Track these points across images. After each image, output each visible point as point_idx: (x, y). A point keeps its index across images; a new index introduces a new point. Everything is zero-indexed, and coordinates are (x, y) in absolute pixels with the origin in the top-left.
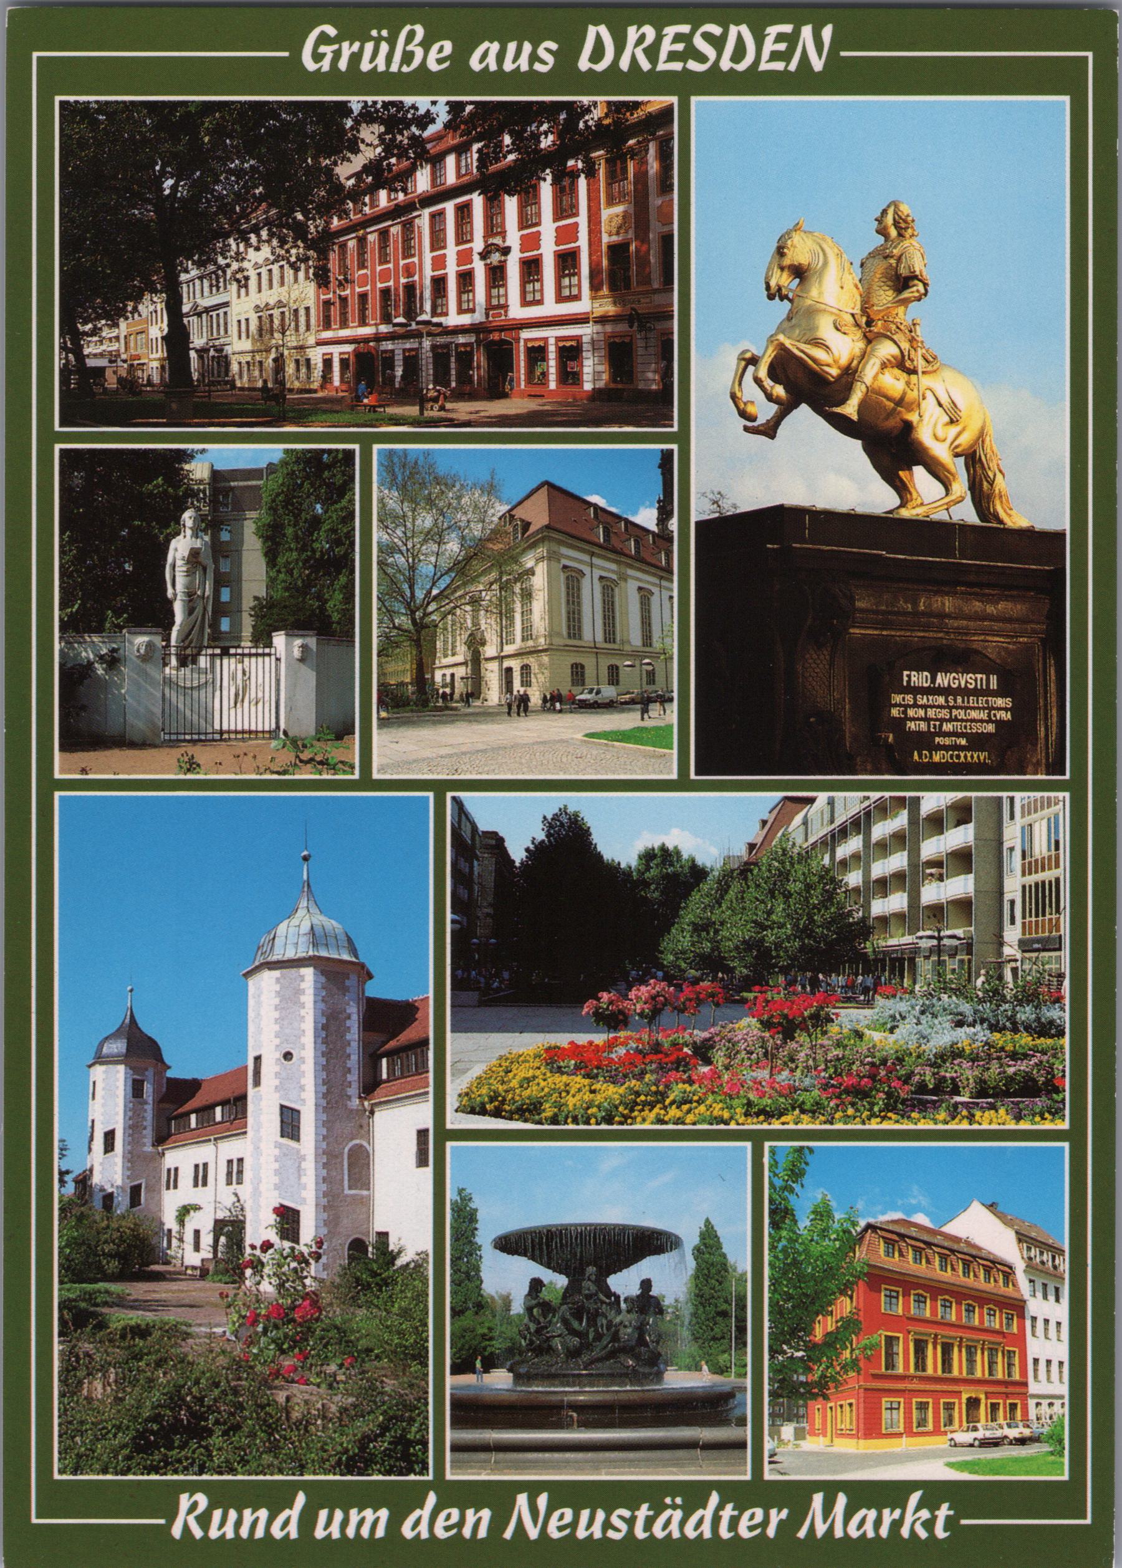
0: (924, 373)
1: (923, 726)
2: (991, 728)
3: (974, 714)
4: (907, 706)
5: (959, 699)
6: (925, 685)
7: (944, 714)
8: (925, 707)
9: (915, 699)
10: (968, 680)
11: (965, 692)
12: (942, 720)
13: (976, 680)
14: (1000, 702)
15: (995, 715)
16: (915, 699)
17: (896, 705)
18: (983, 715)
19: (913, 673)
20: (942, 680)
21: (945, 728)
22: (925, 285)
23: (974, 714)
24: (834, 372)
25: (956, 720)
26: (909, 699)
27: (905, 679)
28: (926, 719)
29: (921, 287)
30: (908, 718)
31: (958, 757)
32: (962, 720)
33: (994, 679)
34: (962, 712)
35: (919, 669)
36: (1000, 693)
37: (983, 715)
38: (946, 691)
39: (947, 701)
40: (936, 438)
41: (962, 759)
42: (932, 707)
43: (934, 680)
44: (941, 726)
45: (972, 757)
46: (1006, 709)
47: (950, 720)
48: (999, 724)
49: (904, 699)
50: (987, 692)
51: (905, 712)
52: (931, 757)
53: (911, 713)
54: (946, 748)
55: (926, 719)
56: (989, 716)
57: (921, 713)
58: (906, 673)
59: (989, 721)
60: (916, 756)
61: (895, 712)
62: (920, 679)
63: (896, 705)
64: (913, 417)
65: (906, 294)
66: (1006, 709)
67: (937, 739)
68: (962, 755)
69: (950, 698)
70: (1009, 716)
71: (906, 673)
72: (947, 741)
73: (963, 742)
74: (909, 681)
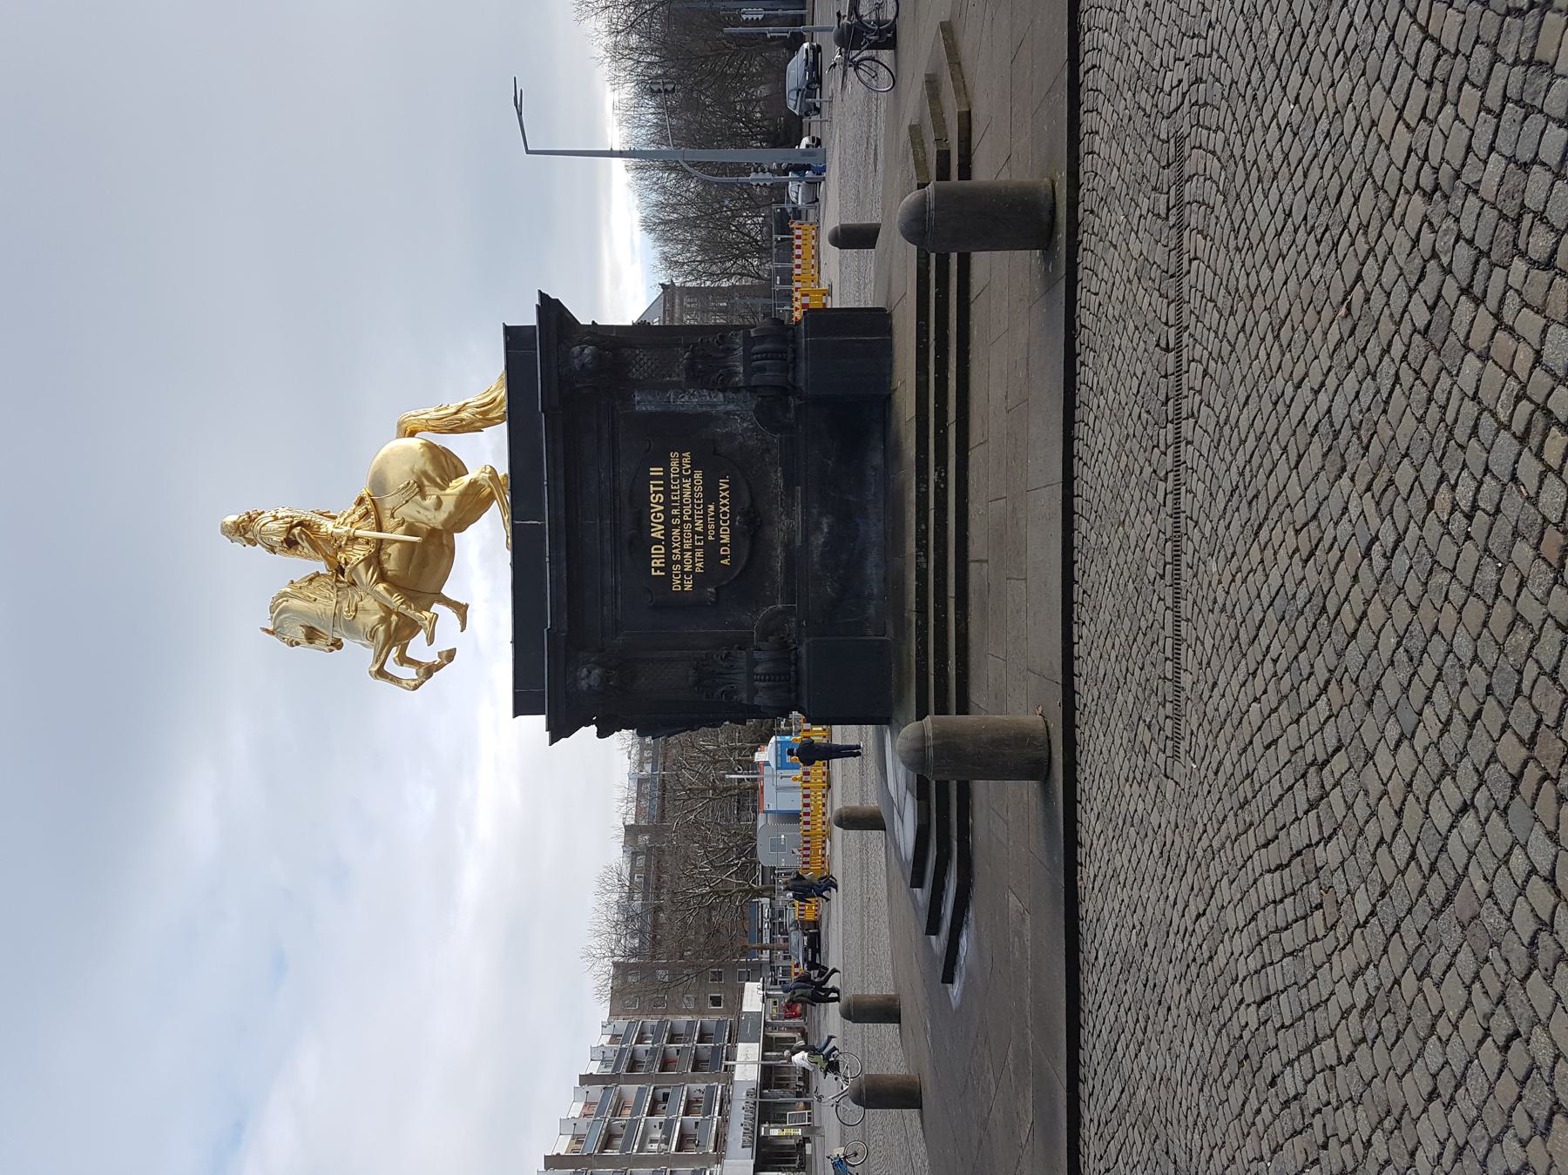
1: (699, 554)
2: (698, 475)
3: (687, 495)
4: (683, 573)
5: (674, 512)
8: (683, 551)
9: (677, 562)
10: (656, 499)
11: (667, 504)
12: (694, 532)
14: (674, 464)
16: (677, 562)
18: (687, 484)
23: (687, 495)
26: (676, 568)
29: (296, 531)
30: (693, 572)
31: (725, 514)
33: (656, 471)
37: (687, 484)
39: (676, 526)
40: (439, 504)
43: (658, 541)
44: (699, 534)
46: (681, 458)
47: (693, 522)
50: (666, 477)
51: (688, 574)
56: (687, 477)
59: (691, 476)
66: (681, 458)
72: (711, 527)
73: (712, 507)
74: (661, 569)
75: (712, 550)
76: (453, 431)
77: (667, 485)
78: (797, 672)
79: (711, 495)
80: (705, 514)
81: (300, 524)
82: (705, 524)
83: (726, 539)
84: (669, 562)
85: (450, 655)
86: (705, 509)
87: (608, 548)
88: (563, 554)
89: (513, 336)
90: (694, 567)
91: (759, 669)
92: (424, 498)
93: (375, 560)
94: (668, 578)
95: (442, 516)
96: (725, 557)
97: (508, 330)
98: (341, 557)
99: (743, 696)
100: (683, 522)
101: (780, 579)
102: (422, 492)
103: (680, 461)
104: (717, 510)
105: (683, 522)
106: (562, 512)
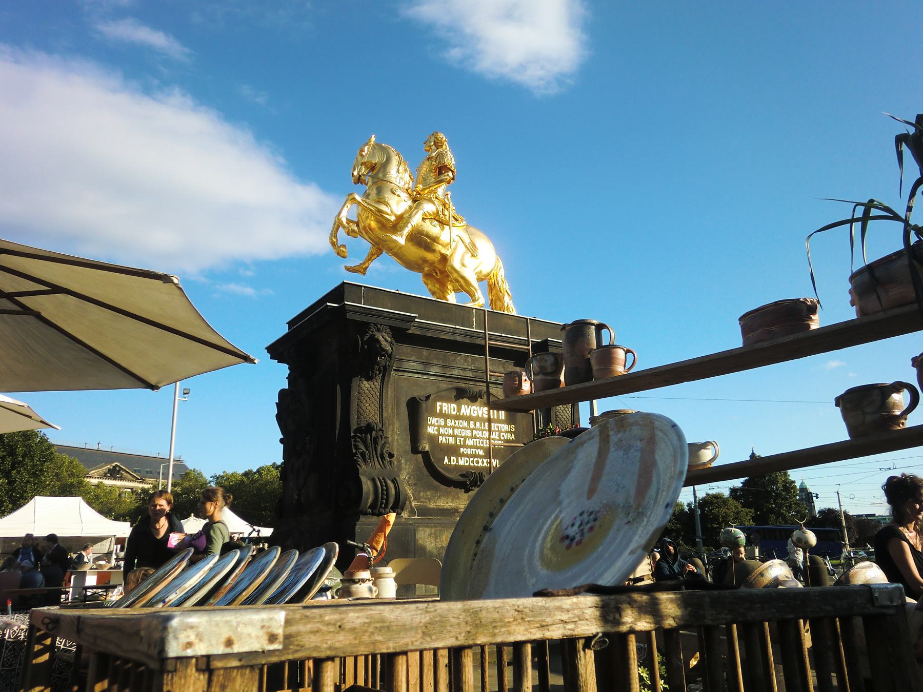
1: (451, 440)
4: (439, 426)
6: (454, 413)
7: (468, 433)
8: (453, 428)
12: (465, 438)
14: (505, 427)
17: (431, 425)
19: (444, 404)
21: (467, 442)
22: (453, 172)
24: (393, 218)
25: (475, 437)
26: (442, 422)
27: (438, 408)
28: (455, 436)
30: (439, 434)
31: (477, 462)
32: (480, 438)
34: (480, 433)
35: (448, 400)
38: (468, 419)
39: (469, 424)
40: (463, 265)
41: (480, 464)
43: (459, 410)
44: (465, 441)
47: (472, 437)
51: (438, 430)
52: (457, 461)
53: (442, 431)
55: (454, 436)
57: (451, 432)
58: (438, 404)
59: (500, 439)
60: (446, 460)
61: (431, 430)
62: (448, 407)
63: (431, 425)
64: (447, 252)
65: (442, 177)
66: (511, 432)
67: (462, 450)
68: (480, 461)
69: (472, 423)
70: (513, 437)
71: (438, 404)
73: (481, 452)
74: (441, 410)
75: (453, 450)
80: (477, 448)
82: (471, 447)
84: (446, 416)
87: (455, 372)
88: (458, 338)
94: (434, 414)
96: (450, 460)
99: (363, 468)
101: (431, 505)
104: (480, 457)
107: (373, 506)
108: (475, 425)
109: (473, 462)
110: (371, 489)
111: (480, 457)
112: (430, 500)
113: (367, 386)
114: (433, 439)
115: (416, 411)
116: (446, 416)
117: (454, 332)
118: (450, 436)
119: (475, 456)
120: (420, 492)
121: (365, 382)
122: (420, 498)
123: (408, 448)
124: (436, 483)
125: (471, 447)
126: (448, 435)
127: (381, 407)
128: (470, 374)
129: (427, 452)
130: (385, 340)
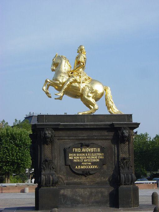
0: (82, 83)
1: (79, 161)
2: (98, 160)
3: (93, 157)
4: (74, 156)
5: (89, 154)
8: (79, 156)
9: (76, 155)
11: (91, 153)
12: (84, 159)
13: (94, 150)
15: (99, 157)
16: (76, 155)
20: (84, 150)
21: (85, 161)
23: (93, 157)
24: (61, 85)
25: (88, 159)
26: (75, 155)
29: (82, 64)
31: (89, 167)
32: (90, 159)
33: (99, 150)
36: (101, 152)
38: (85, 153)
39: (85, 155)
40: (88, 96)
42: (81, 156)
43: (81, 150)
44: (83, 161)
45: (93, 167)
47: (86, 159)
48: (100, 159)
49: (73, 155)
52: (81, 167)
54: (85, 165)
56: (97, 157)
58: (73, 149)
59: (98, 159)
63: (71, 156)
72: (85, 164)
73: (90, 164)
75: (79, 164)
76: (106, 99)
77: (95, 152)
78: (50, 186)
79: (93, 163)
80: (88, 162)
81: (84, 64)
82: (86, 162)
83: (82, 168)
84: (76, 153)
85: (50, 97)
86: (90, 162)
89: (130, 116)
90: (75, 159)
91: (50, 176)
92: (90, 93)
93: (75, 81)
95: (86, 97)
96: (78, 167)
97: (131, 115)
98: (76, 73)
99: (43, 172)
100: (86, 156)
102: (92, 93)
103: (101, 156)
104: (90, 165)
105: (86, 156)
106: (88, 127)
107: (45, 184)
108: (88, 154)
109: (87, 167)
110: (45, 179)
111: (90, 165)
112: (71, 180)
113: (47, 147)
114: (72, 160)
115: (66, 153)
116: (76, 153)
117: (77, 125)
118: (78, 159)
119: (88, 165)
120: (68, 178)
121: (46, 146)
122: (68, 179)
123: (64, 164)
124: (73, 174)
125: (86, 162)
126: (77, 159)
127: (52, 153)
128: (86, 138)
129: (70, 165)
130: (48, 133)
